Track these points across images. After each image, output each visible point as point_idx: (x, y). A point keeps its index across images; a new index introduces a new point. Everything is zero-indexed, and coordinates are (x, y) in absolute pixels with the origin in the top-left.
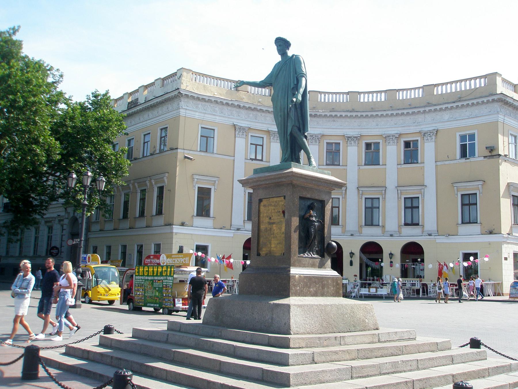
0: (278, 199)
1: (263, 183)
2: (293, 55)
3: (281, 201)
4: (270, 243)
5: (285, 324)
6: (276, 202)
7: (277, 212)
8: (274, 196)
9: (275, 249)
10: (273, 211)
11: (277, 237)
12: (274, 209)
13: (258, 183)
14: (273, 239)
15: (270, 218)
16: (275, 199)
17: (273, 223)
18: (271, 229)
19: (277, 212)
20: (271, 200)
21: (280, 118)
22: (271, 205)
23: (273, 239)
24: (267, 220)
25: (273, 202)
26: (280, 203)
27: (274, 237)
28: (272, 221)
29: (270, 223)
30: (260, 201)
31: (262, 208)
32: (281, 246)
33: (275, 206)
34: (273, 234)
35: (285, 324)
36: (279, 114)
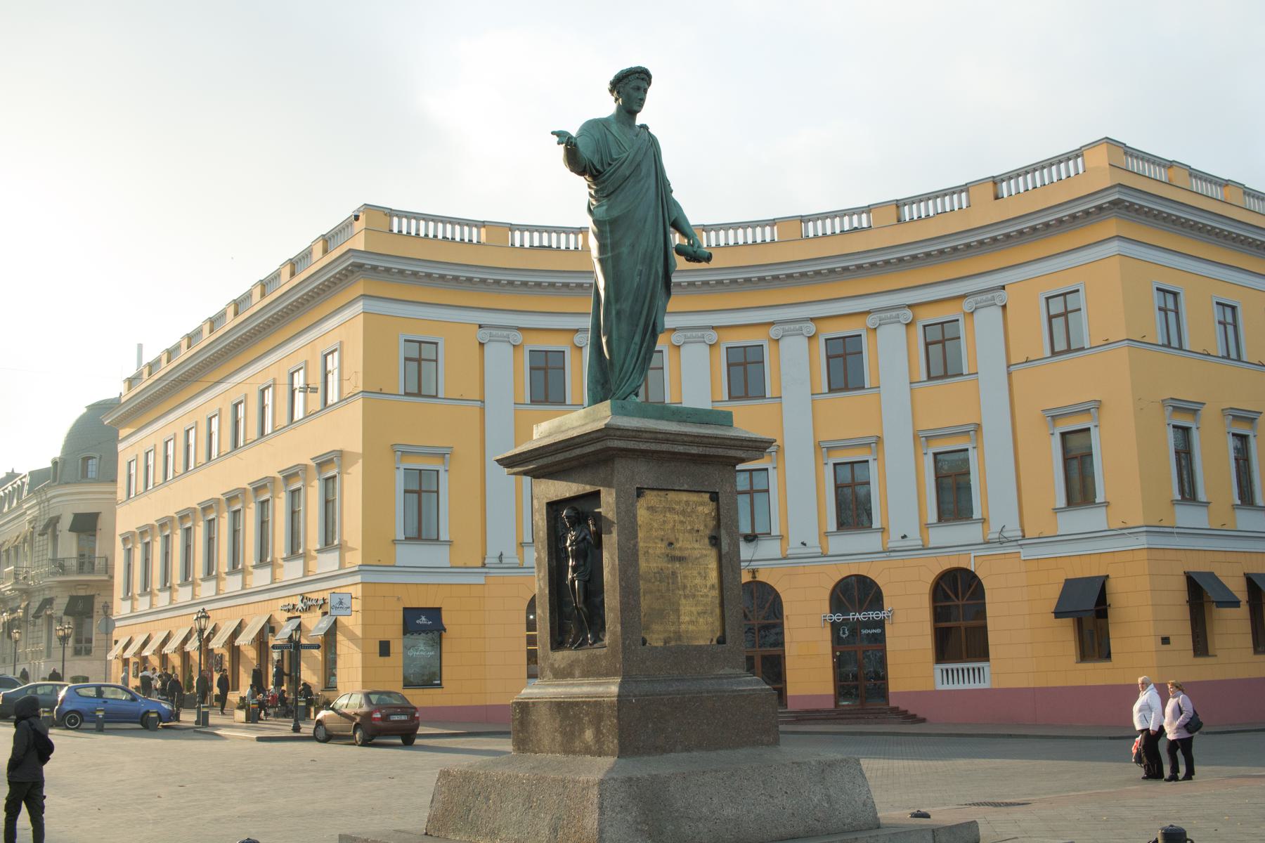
0: (694, 498)
1: (681, 449)
2: (644, 127)
3: (702, 504)
4: (677, 611)
5: (864, 805)
6: (687, 503)
7: (690, 531)
8: (686, 487)
9: (691, 627)
10: (678, 526)
11: (694, 596)
12: (681, 522)
13: (664, 447)
14: (683, 601)
15: (671, 544)
16: (684, 497)
17: (681, 559)
18: (674, 573)
19: (690, 531)
20: (671, 495)
21: (637, 279)
22: (671, 510)
23: (683, 601)
24: (661, 547)
25: (679, 503)
26: (700, 509)
27: (686, 597)
28: (678, 553)
29: (674, 559)
30: (640, 492)
31: (642, 514)
32: (710, 620)
33: (683, 513)
34: (685, 587)
35: (864, 805)
36: (639, 267)
